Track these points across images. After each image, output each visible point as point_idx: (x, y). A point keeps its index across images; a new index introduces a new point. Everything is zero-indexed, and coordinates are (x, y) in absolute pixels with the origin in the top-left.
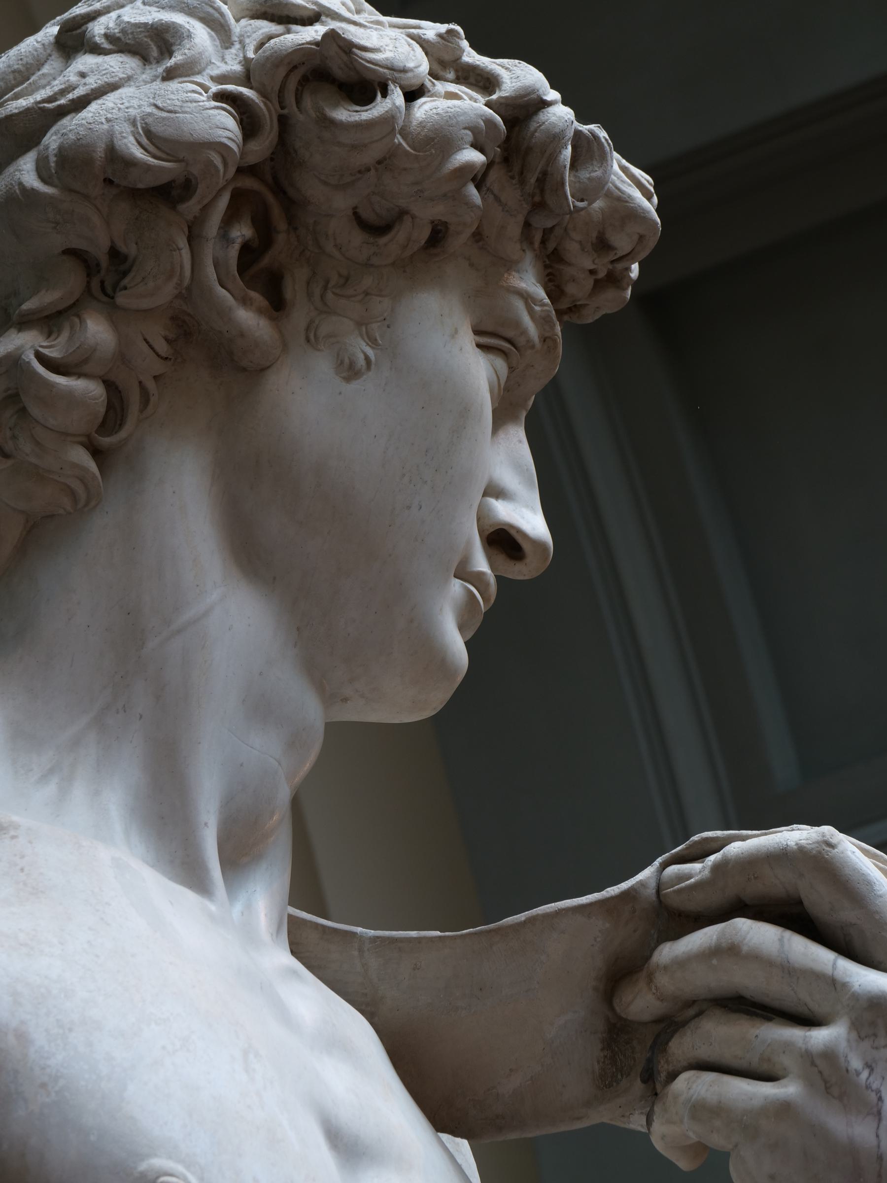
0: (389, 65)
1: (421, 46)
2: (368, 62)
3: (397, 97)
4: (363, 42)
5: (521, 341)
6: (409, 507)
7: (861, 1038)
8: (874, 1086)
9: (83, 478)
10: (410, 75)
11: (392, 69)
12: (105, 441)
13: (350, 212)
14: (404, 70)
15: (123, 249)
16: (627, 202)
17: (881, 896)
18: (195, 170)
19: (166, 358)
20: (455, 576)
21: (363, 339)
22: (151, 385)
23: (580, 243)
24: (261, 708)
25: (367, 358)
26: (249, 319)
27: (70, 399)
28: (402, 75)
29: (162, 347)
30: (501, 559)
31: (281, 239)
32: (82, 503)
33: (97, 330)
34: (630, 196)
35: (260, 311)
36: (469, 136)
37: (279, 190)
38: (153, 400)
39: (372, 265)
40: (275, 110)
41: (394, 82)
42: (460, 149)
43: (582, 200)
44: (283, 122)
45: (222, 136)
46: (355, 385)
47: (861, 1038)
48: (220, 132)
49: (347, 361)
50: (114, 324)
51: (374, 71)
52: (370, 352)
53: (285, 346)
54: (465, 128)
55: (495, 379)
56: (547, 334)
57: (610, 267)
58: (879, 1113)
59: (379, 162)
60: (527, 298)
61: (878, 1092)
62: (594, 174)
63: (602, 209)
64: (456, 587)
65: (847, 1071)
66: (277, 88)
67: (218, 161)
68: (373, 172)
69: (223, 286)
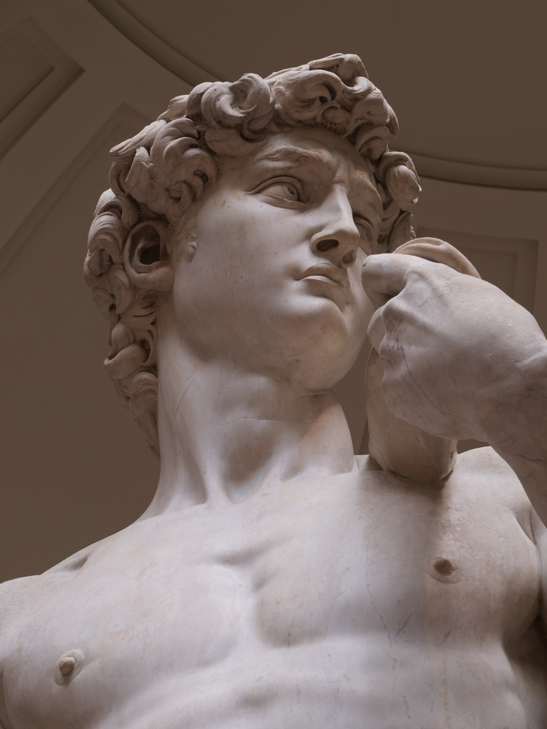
0: (133, 144)
1: (164, 119)
3: (142, 152)
5: (278, 173)
7: (391, 332)
9: (146, 382)
11: (135, 144)
12: (147, 363)
13: (171, 201)
18: (101, 247)
20: (298, 280)
21: (190, 241)
23: (296, 111)
24: (225, 405)
26: (156, 274)
28: (141, 142)
29: (144, 312)
31: (162, 233)
32: (153, 391)
33: (118, 330)
35: (157, 267)
36: (169, 138)
37: (149, 219)
39: (185, 211)
41: (138, 147)
44: (130, 198)
47: (391, 332)
49: (187, 255)
52: (194, 244)
54: (163, 138)
55: (268, 198)
56: (296, 158)
57: (335, 101)
58: (404, 355)
61: (402, 346)
63: (291, 93)
64: (296, 285)
66: (118, 188)
67: (103, 237)
68: (154, 183)
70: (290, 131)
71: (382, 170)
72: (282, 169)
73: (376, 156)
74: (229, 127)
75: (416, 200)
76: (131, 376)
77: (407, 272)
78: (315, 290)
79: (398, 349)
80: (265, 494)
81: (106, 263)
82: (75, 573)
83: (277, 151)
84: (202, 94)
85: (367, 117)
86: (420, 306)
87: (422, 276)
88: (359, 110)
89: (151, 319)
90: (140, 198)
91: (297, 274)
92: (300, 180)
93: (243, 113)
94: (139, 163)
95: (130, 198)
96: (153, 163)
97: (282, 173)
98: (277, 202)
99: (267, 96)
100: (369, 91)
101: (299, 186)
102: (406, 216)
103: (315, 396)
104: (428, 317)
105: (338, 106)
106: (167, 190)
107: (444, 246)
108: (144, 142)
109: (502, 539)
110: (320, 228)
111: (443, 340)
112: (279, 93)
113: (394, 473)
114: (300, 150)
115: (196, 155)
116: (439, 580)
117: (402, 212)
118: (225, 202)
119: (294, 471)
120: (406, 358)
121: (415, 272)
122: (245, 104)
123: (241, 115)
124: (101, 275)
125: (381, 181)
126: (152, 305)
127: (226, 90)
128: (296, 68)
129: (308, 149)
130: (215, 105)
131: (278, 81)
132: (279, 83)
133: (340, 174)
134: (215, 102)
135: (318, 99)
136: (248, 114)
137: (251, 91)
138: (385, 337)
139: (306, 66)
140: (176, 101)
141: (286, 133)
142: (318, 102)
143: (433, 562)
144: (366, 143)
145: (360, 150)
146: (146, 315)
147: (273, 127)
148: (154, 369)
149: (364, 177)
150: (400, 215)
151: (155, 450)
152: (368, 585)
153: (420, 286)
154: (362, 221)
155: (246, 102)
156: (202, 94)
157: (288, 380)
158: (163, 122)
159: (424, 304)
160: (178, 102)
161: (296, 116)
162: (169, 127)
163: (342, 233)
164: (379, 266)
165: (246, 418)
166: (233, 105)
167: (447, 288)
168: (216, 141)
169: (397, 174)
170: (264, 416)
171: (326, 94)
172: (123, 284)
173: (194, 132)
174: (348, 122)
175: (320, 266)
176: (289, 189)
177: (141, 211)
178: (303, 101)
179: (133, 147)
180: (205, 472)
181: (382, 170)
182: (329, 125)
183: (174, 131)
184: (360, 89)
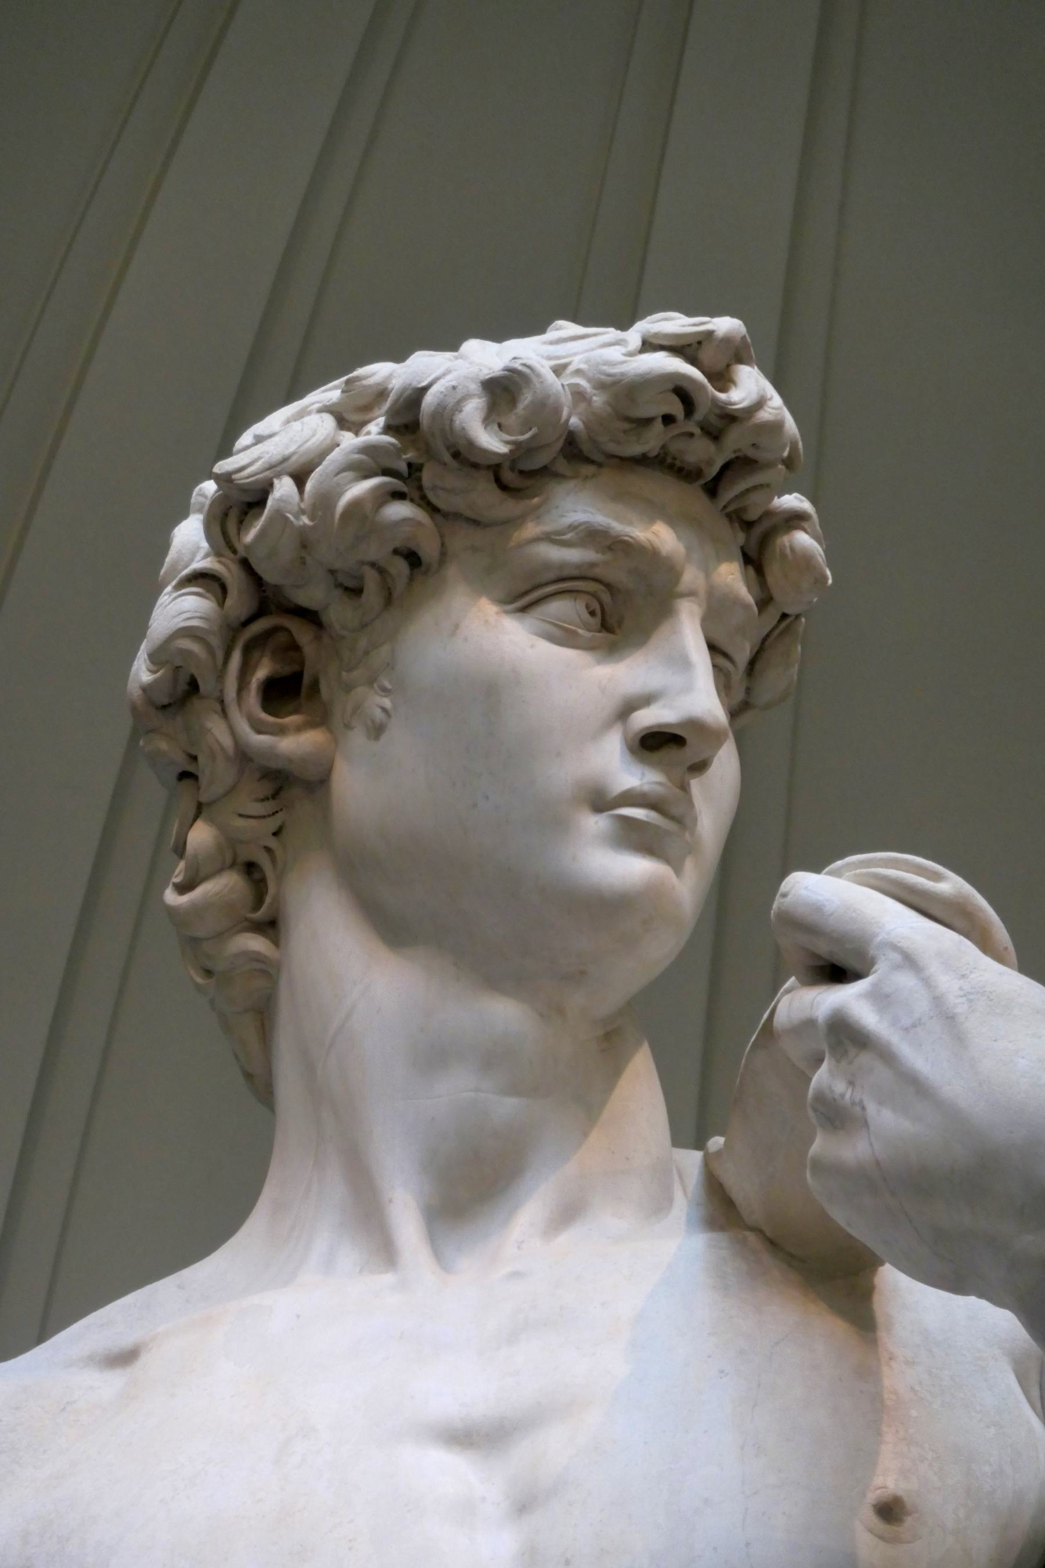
0: (267, 466)
2: (248, 478)
3: (284, 488)
4: (236, 466)
5: (566, 573)
6: (475, 806)
8: (857, 1100)
9: (257, 958)
10: (294, 458)
11: (271, 467)
12: (260, 915)
13: (338, 592)
14: (285, 459)
15: (194, 753)
16: (620, 381)
17: (832, 914)
18: (178, 663)
19: (274, 814)
21: (376, 693)
22: (272, 843)
24: (433, 1056)
25: (384, 710)
26: (295, 742)
27: (197, 911)
28: (285, 465)
29: (259, 809)
30: (671, 753)
33: (201, 836)
34: (622, 374)
35: (299, 729)
36: (349, 475)
38: (279, 853)
40: (232, 560)
41: (279, 475)
42: (341, 494)
43: (530, 429)
44: (245, 564)
45: (180, 623)
46: (385, 737)
47: (838, 1061)
48: (176, 620)
49: (370, 723)
50: (211, 821)
51: (256, 481)
52: (387, 702)
53: (336, 741)
54: (338, 474)
58: (866, 1121)
59: (304, 546)
60: (549, 538)
61: (861, 1101)
62: (526, 402)
64: (596, 824)
65: (835, 1100)
68: (309, 559)
69: (259, 732)
70: (594, 476)
71: (758, 544)
72: (578, 566)
73: (752, 515)
74: (475, 466)
75: (815, 600)
76: (221, 936)
77: (879, 939)
78: (634, 838)
79: (853, 1103)
80: (516, 1275)
81: (182, 686)
82: (113, 1381)
83: (570, 526)
84: (425, 389)
85: (750, 453)
86: (906, 1030)
87: (909, 961)
88: (735, 441)
89: (272, 824)
90: (270, 576)
91: (600, 801)
92: (608, 586)
93: (507, 443)
94: (279, 515)
95: (245, 564)
96: (312, 519)
97: (575, 573)
98: (565, 638)
99: (557, 410)
100: (760, 404)
101: (606, 598)
102: (792, 622)
103: (608, 1036)
104: (921, 1057)
105: (697, 431)
106: (332, 572)
107: (951, 884)
108: (293, 464)
109: (993, 1430)
110: (647, 700)
111: (951, 1115)
112: (578, 395)
113: (773, 1244)
114: (618, 527)
115: (405, 520)
116: (881, 1537)
117: (784, 616)
118: (457, 626)
119: (568, 1213)
120: (871, 1128)
121: (895, 947)
122: (511, 420)
123: (502, 448)
124: (164, 707)
125: (754, 561)
126: (275, 796)
127: (474, 387)
128: (611, 333)
129: (630, 523)
130: (452, 421)
131: (577, 363)
132: (578, 372)
133: (691, 576)
134: (453, 415)
135: (660, 420)
136: (517, 444)
137: (526, 399)
138: (825, 1066)
139: (634, 336)
140: (358, 379)
141: (587, 477)
142: (658, 425)
143: (872, 1497)
144: (737, 497)
145: (725, 507)
146: (264, 817)
147: (562, 466)
148: (271, 927)
149: (731, 576)
150: (780, 621)
151: (262, 1088)
152: (748, 1544)
153: (905, 981)
154: (722, 661)
155: (513, 417)
156: (425, 389)
157: (561, 1011)
158: (328, 422)
159: (914, 1026)
160: (364, 382)
161: (612, 448)
162: (352, 452)
163: (696, 725)
164: (818, 908)
165: (477, 1090)
166: (487, 421)
167: (960, 1000)
168: (443, 489)
169: (788, 551)
170: (513, 1089)
171: (676, 408)
172: (223, 749)
173: (403, 467)
174: (710, 463)
175: (646, 788)
176: (587, 607)
177: (264, 591)
178: (628, 419)
179: (267, 473)
180: (390, 1201)
181: (758, 544)
182: (669, 460)
183: (361, 462)
184: (743, 400)
